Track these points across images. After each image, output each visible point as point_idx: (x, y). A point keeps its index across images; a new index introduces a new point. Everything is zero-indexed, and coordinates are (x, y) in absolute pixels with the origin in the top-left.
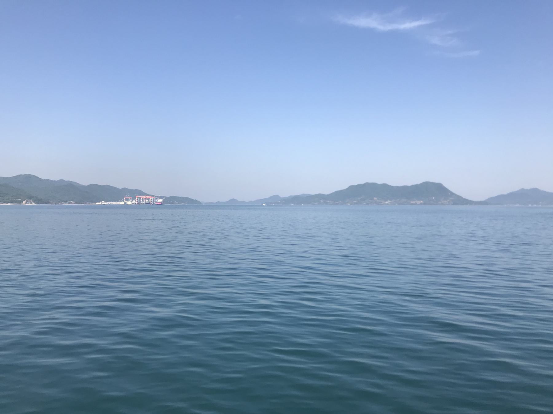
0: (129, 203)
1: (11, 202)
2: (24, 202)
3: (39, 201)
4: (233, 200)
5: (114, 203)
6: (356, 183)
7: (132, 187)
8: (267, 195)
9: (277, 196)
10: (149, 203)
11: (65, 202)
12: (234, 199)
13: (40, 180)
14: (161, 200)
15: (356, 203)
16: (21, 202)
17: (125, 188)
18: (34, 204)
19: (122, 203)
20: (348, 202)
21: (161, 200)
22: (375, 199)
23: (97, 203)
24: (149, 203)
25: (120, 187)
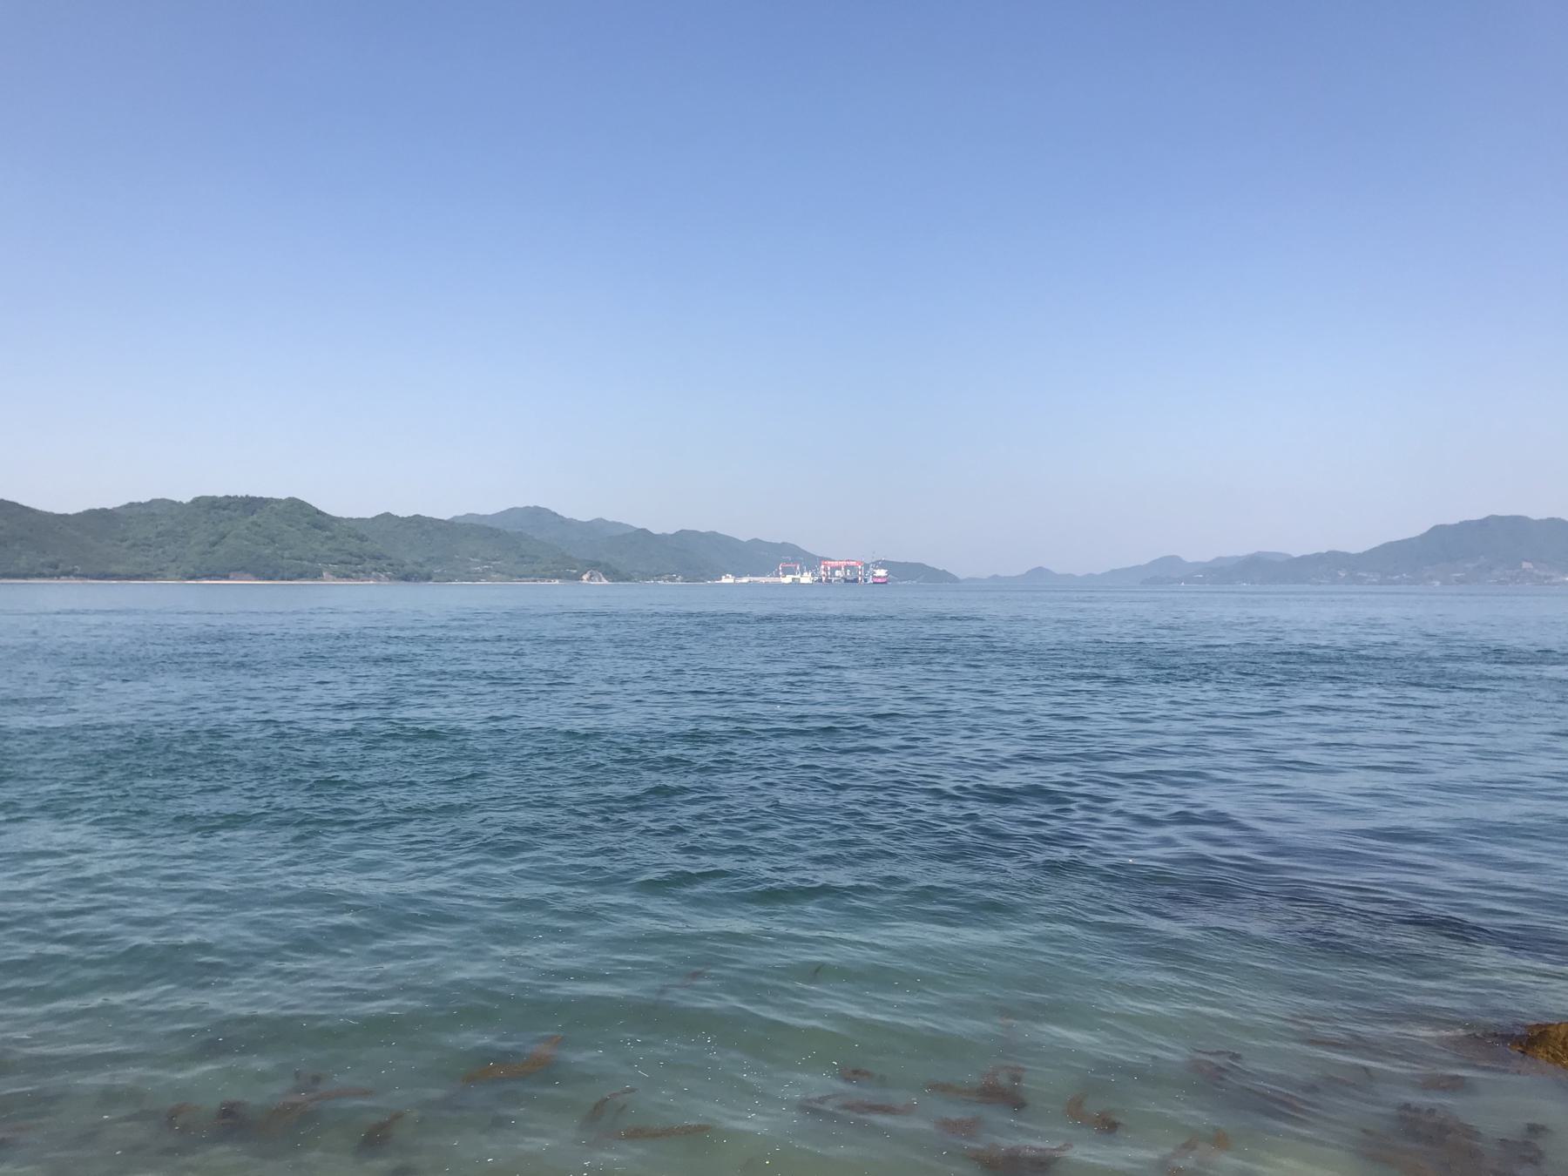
0: (803, 580)
1: (559, 577)
2: (585, 577)
3: (614, 574)
4: (1040, 572)
5: (762, 580)
6: (1452, 519)
7: (772, 534)
8: (1141, 554)
9: (1172, 561)
10: (856, 580)
11: (659, 576)
12: (1040, 568)
13: (563, 522)
14: (881, 573)
15: (1460, 581)
16: (578, 577)
17: (756, 540)
18: (605, 582)
19: (788, 579)
20: (1431, 578)
21: (881, 573)
22: (1525, 565)
23: (724, 580)
24: (856, 580)
25: (744, 537)
